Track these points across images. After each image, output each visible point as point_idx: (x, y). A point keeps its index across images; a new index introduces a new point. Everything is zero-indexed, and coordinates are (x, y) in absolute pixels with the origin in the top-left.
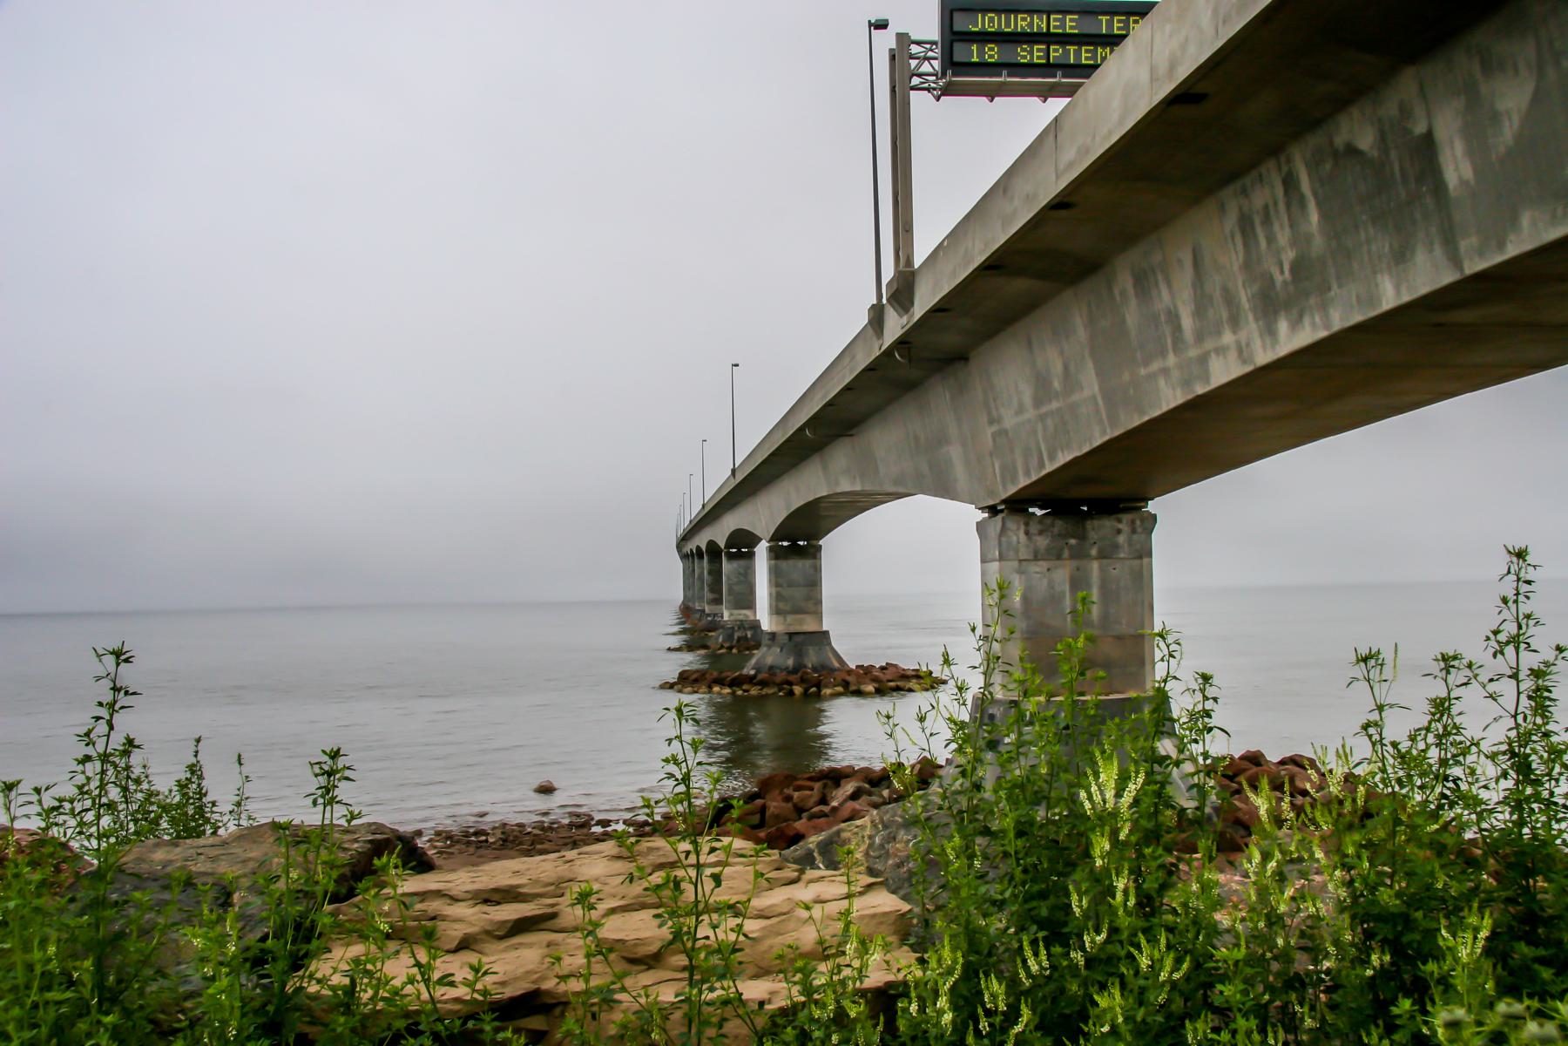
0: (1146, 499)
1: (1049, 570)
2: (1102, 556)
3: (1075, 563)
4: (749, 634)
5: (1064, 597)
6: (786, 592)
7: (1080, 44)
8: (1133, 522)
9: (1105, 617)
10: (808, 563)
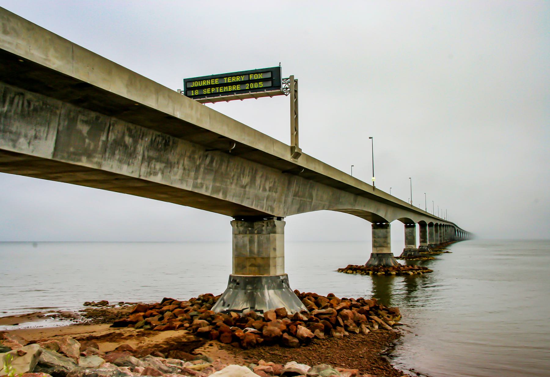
1: (243, 237)
2: (258, 233)
4: (413, 253)
5: (247, 245)
6: (377, 240)
7: (219, 87)
8: (267, 223)
9: (259, 252)
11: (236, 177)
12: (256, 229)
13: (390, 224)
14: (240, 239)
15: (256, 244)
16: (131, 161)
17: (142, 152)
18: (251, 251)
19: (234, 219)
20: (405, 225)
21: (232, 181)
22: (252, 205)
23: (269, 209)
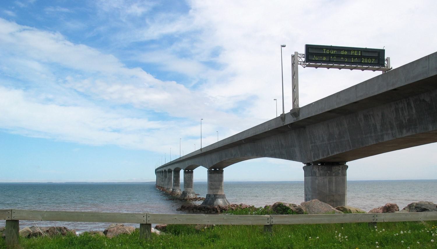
0: (345, 162)
2: (336, 175)
8: (343, 167)
12: (334, 172)
14: (321, 180)
19: (306, 165)
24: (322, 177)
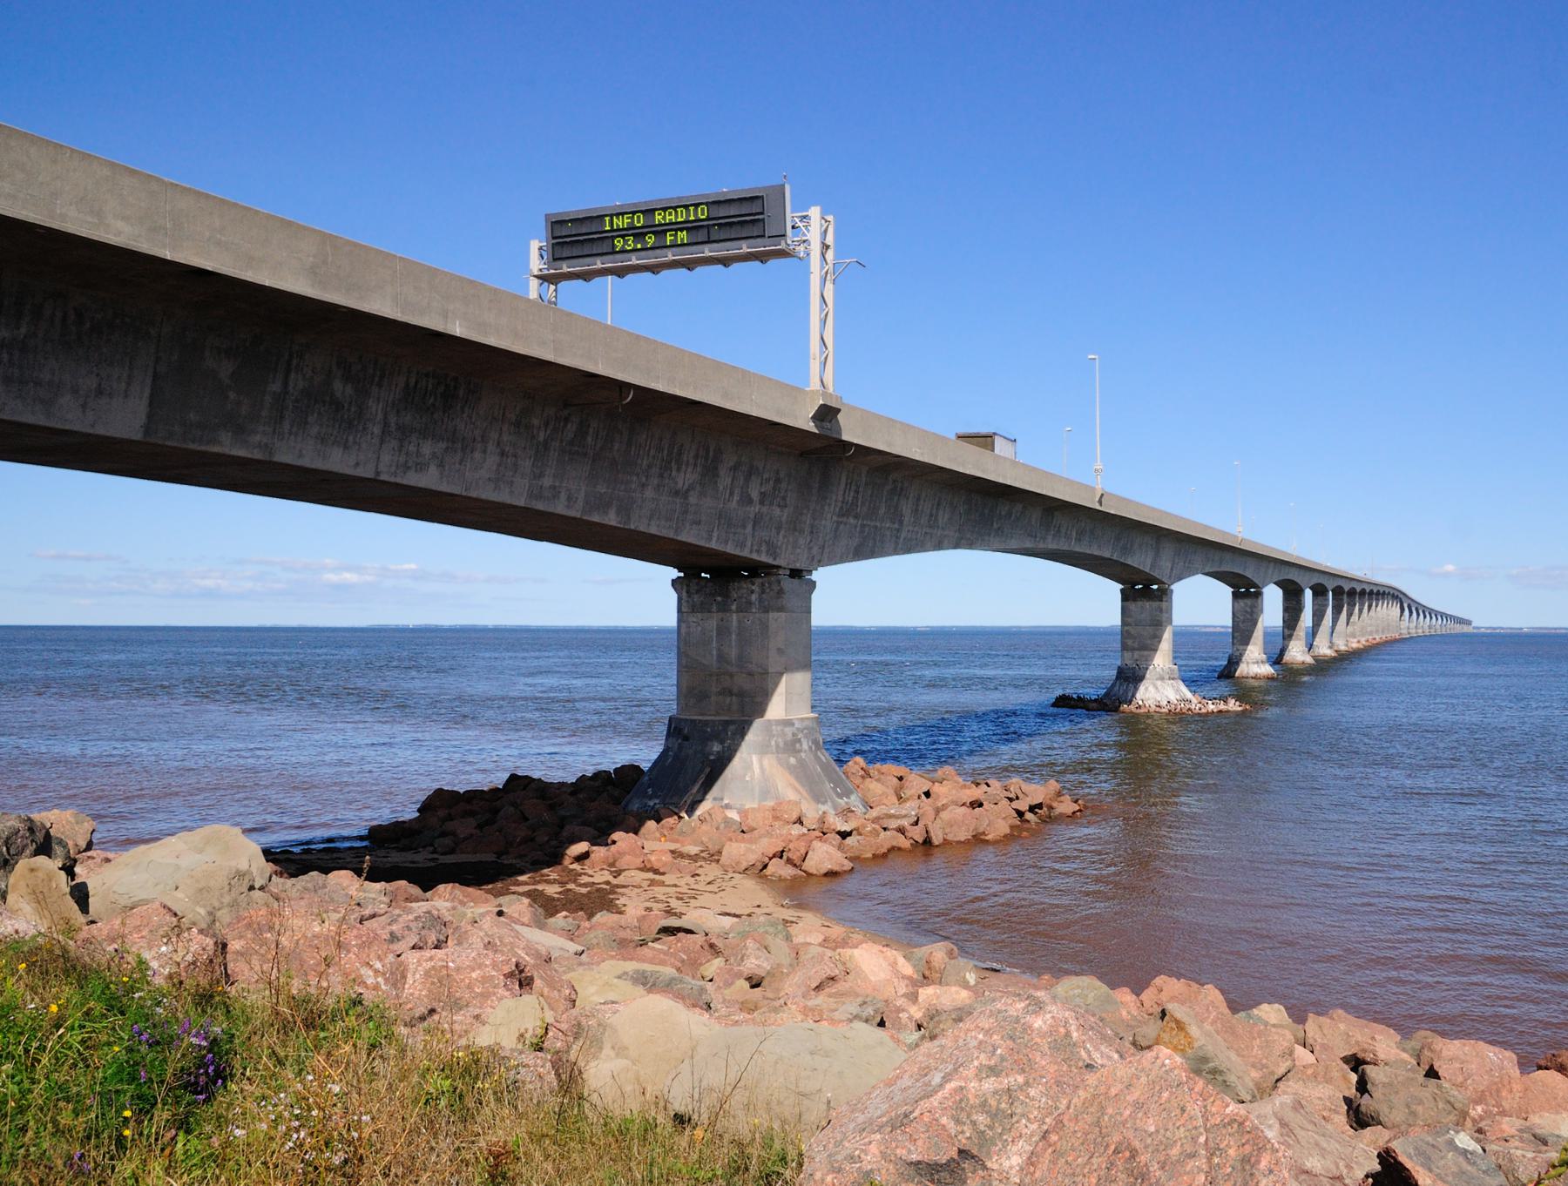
2: (740, 610)
3: (721, 615)
6: (1132, 630)
8: (763, 584)
10: (1155, 604)
11: (655, 470)
13: (1173, 587)
15: (734, 636)
16: (351, 438)
17: (380, 416)
18: (721, 657)
19: (682, 575)
20: (1122, 591)
21: (644, 479)
22: (710, 539)
23: (764, 548)
24: (699, 615)
